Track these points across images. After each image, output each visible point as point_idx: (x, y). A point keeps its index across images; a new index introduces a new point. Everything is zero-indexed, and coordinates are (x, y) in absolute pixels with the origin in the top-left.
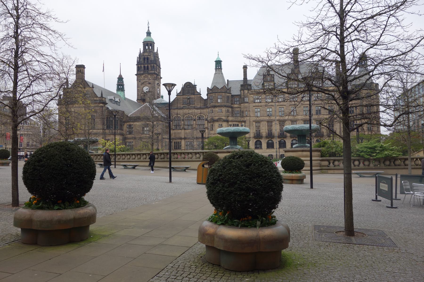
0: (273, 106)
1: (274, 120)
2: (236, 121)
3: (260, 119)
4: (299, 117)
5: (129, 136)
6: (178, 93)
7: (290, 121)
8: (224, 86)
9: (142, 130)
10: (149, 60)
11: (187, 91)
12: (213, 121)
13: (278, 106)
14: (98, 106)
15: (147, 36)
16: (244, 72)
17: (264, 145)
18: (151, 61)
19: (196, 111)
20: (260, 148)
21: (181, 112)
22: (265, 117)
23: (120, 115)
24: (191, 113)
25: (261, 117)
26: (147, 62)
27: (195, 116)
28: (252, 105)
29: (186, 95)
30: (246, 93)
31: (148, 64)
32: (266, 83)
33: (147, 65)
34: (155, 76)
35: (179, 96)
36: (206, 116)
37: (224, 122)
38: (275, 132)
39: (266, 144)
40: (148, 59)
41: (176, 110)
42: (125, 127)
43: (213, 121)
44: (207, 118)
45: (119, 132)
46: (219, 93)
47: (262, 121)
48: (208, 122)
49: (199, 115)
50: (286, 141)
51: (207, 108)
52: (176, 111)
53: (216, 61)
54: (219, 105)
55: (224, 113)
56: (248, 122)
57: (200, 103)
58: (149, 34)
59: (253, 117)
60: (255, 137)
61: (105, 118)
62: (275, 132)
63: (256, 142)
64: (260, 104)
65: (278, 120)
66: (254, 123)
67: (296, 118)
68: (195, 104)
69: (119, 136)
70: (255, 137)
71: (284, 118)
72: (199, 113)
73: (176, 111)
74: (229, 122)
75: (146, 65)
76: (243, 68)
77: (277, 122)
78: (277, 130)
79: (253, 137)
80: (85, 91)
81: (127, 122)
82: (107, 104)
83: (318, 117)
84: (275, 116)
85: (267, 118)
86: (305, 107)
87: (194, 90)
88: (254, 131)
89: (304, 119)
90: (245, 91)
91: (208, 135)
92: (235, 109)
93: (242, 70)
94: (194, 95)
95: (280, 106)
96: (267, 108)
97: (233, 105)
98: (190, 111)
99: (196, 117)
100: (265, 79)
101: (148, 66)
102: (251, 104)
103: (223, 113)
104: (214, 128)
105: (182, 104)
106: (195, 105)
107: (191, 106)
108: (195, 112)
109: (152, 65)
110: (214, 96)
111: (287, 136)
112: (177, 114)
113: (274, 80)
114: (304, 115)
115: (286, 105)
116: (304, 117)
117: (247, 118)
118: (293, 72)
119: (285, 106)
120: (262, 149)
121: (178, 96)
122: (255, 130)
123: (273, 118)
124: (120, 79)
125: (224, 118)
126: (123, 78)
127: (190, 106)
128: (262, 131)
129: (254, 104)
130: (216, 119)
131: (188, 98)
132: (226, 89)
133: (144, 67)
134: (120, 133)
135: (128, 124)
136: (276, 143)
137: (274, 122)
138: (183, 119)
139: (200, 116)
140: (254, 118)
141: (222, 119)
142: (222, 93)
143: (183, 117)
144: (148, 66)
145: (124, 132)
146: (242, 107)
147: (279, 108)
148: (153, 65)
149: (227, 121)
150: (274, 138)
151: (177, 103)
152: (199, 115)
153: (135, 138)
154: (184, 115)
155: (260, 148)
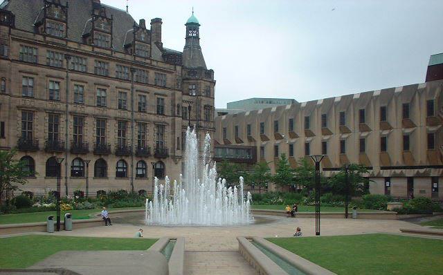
0: (63, 79)
47: (38, 110)
50: (108, 163)
56: (7, 109)
78: (69, 136)
79: (16, 147)
96: (50, 81)
100: (47, 13)
128: (37, 134)
136: (66, 164)
147: (75, 85)
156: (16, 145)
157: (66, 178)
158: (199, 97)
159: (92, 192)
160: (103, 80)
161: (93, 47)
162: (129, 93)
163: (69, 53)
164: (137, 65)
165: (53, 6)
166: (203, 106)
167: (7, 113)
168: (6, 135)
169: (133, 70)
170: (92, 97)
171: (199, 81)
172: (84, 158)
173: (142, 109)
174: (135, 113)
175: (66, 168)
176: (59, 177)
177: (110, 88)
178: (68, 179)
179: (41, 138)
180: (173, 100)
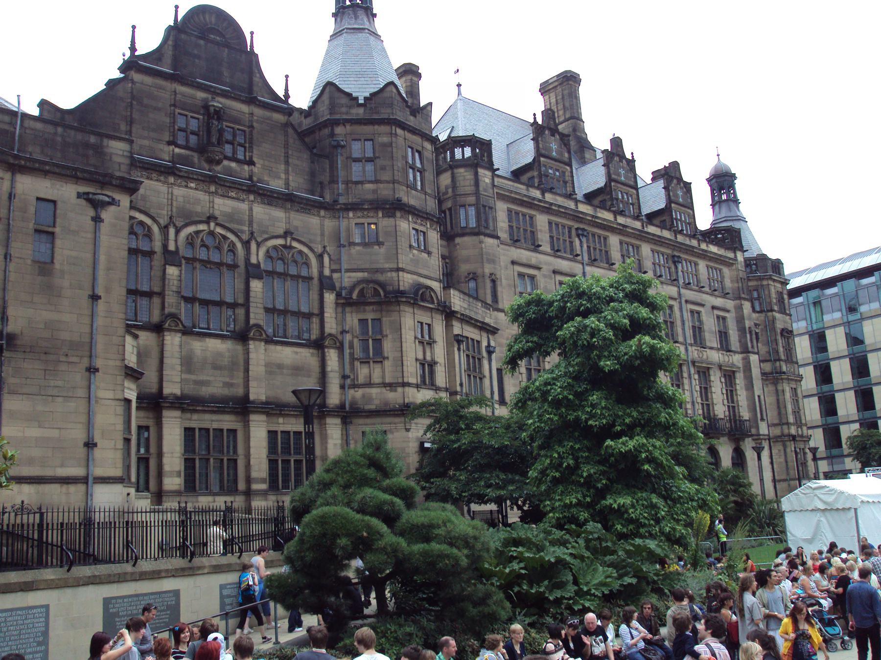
19: (260, 211)
24: (231, 217)
35: (148, 80)
48: (345, 302)
49: (281, 242)
57: (283, 167)
68: (251, 163)
72: (281, 232)
91: (342, 387)
98: (218, 201)
104: (388, 346)
106: (255, 170)
108: (251, 216)
110: (385, 139)
121: (137, 77)
143: (172, 231)
151: (131, 122)
152: (281, 242)
154: (179, 224)
158: (770, 314)
161: (615, 214)
162: (676, 304)
166: (779, 331)
171: (765, 283)
173: (699, 339)
180: (740, 320)
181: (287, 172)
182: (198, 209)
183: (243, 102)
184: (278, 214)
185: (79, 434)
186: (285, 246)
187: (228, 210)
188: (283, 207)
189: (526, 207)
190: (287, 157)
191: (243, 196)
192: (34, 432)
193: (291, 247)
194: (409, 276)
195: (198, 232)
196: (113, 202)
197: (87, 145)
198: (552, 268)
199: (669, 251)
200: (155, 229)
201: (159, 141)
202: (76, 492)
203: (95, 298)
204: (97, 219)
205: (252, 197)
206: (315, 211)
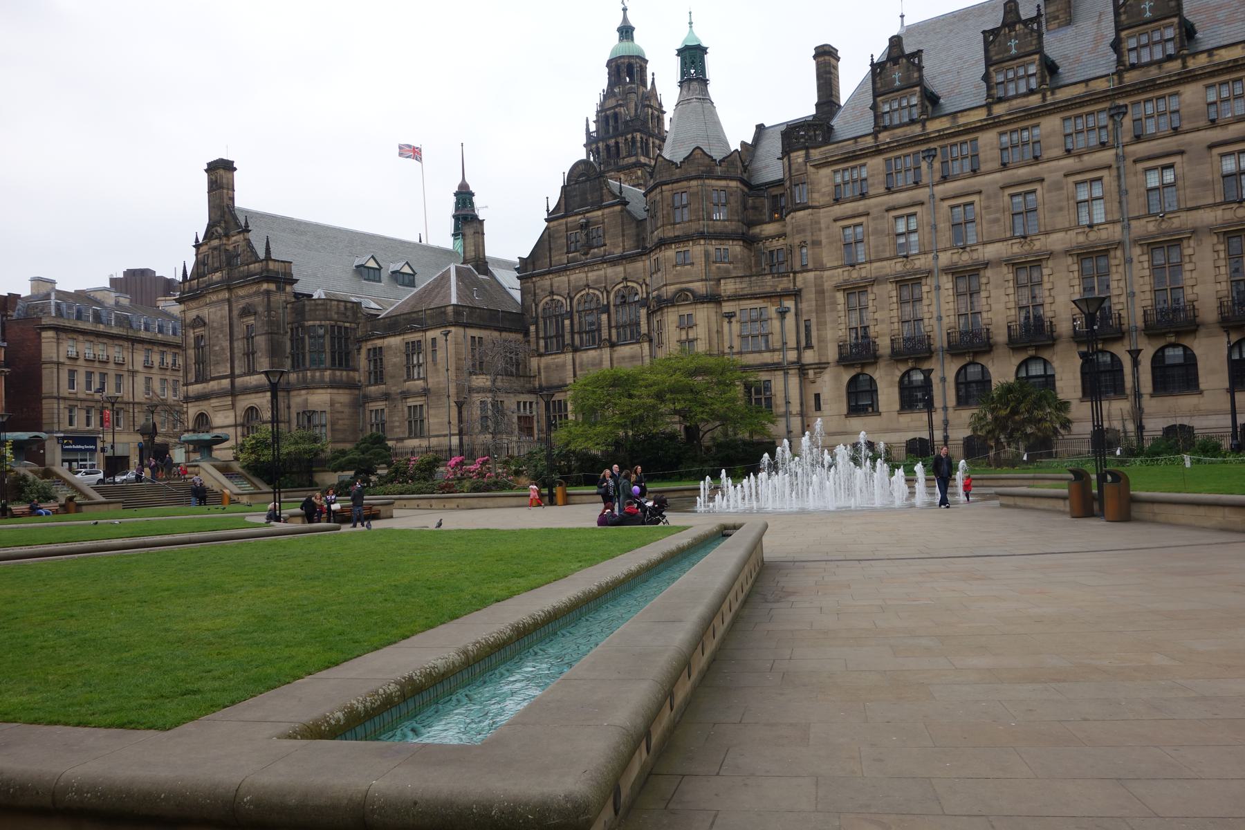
0: (922, 204)
1: (929, 273)
2: (754, 297)
3: (864, 274)
4: (1057, 241)
5: (373, 388)
6: (551, 209)
7: (1005, 269)
8: (698, 151)
9: (405, 363)
10: (619, 121)
11: (578, 199)
12: (659, 305)
13: (942, 200)
14: (257, 293)
15: (620, 40)
16: (819, 76)
17: (888, 396)
18: (626, 122)
20: (870, 409)
21: (561, 281)
22: (885, 263)
23: (336, 316)
24: (597, 281)
25: (868, 266)
26: (616, 129)
27: (608, 293)
28: (826, 215)
29: (577, 214)
30: (800, 164)
31: (615, 136)
32: (884, 102)
33: (613, 141)
34: (639, 173)
35: (555, 223)
36: (644, 286)
37: (699, 306)
38: (936, 328)
39: (896, 390)
40: (616, 116)
41: (547, 277)
42: (363, 361)
43: (659, 305)
44: (648, 294)
45: (327, 379)
46: (677, 181)
47: (874, 281)
49: (622, 285)
51: (645, 252)
52: (548, 282)
53: (680, 52)
54: (676, 234)
55: (699, 268)
58: (626, 32)
59: (836, 268)
60: (845, 360)
61: (287, 332)
62: (936, 328)
63: (853, 381)
64: (862, 203)
65: (947, 270)
66: (840, 297)
67: (1037, 245)
68: (605, 245)
69: (329, 391)
70: (845, 360)
71: (975, 256)
72: (620, 280)
73: (546, 282)
74: (723, 304)
75: (612, 142)
76: (815, 57)
77: (947, 283)
78: (945, 320)
80: (229, 245)
81: (367, 340)
82: (296, 281)
83: (1164, 226)
84: (931, 252)
85: (897, 267)
86: (1084, 182)
87: (602, 189)
88: (840, 333)
89: (1079, 247)
90: (793, 155)
92: (767, 243)
93: (811, 67)
94: (600, 208)
95: (954, 197)
97: (757, 230)
98: (590, 274)
99: (612, 296)
101: (617, 143)
102: (822, 210)
103: (695, 268)
105: (565, 251)
106: (607, 248)
107: (594, 253)
108: (606, 277)
109: (629, 136)
111: (996, 344)
112: (552, 293)
113: (921, 77)
114: (1083, 227)
115: (982, 188)
116: (1081, 238)
117: (804, 279)
118: (1012, 17)
119: (980, 192)
120: (880, 414)
121: (552, 224)
122: (843, 326)
123: (923, 261)
124: (464, 197)
125: (699, 287)
126: (473, 195)
127: (589, 256)
128: (877, 328)
129: (836, 207)
130: (669, 294)
131: (582, 226)
132: (707, 161)
133: (608, 147)
134: (331, 382)
135: (370, 345)
136: (943, 380)
137: (929, 281)
138: (569, 309)
139: (626, 293)
140: (840, 270)
141: (692, 291)
142: (686, 180)
143: (568, 301)
144: (617, 143)
145: (360, 376)
146: (788, 229)
148: (633, 138)
149: (714, 299)
150: (934, 360)
151: (550, 249)
152: (622, 285)
153: (386, 397)
154: (572, 295)
155: (870, 409)
156: (837, 357)
157: (945, 408)
159: (1155, 425)
160: (1023, 172)
163: (932, 145)
164: (1128, 94)
165: (888, 65)
167: (814, 303)
168: (814, 342)
169: (1117, 113)
170: (997, 221)
172: (983, 360)
174: (1133, 223)
175: (944, 387)
176: (929, 406)
177: (1045, 184)
178: (950, 410)
179: (884, 335)
181: (623, 241)
182: (581, 283)
183: (597, 210)
184: (620, 269)
185: (446, 420)
186: (624, 287)
187: (595, 278)
188: (622, 264)
189: (853, 160)
190: (623, 230)
191: (601, 266)
192: (436, 420)
193: (627, 286)
194: (672, 287)
195: (582, 296)
196: (449, 332)
197: (442, 312)
198: (884, 207)
199: (1106, 105)
200: (564, 301)
201: (562, 254)
202: (447, 438)
203: (447, 370)
204: (446, 340)
205: (605, 265)
206: (639, 258)
